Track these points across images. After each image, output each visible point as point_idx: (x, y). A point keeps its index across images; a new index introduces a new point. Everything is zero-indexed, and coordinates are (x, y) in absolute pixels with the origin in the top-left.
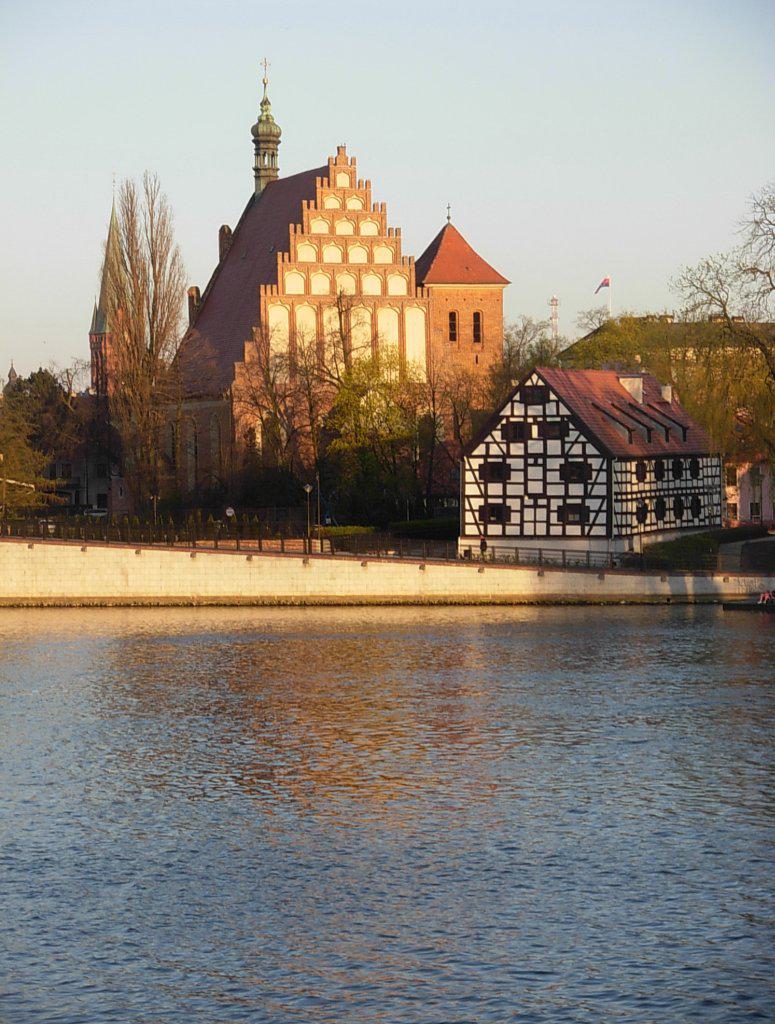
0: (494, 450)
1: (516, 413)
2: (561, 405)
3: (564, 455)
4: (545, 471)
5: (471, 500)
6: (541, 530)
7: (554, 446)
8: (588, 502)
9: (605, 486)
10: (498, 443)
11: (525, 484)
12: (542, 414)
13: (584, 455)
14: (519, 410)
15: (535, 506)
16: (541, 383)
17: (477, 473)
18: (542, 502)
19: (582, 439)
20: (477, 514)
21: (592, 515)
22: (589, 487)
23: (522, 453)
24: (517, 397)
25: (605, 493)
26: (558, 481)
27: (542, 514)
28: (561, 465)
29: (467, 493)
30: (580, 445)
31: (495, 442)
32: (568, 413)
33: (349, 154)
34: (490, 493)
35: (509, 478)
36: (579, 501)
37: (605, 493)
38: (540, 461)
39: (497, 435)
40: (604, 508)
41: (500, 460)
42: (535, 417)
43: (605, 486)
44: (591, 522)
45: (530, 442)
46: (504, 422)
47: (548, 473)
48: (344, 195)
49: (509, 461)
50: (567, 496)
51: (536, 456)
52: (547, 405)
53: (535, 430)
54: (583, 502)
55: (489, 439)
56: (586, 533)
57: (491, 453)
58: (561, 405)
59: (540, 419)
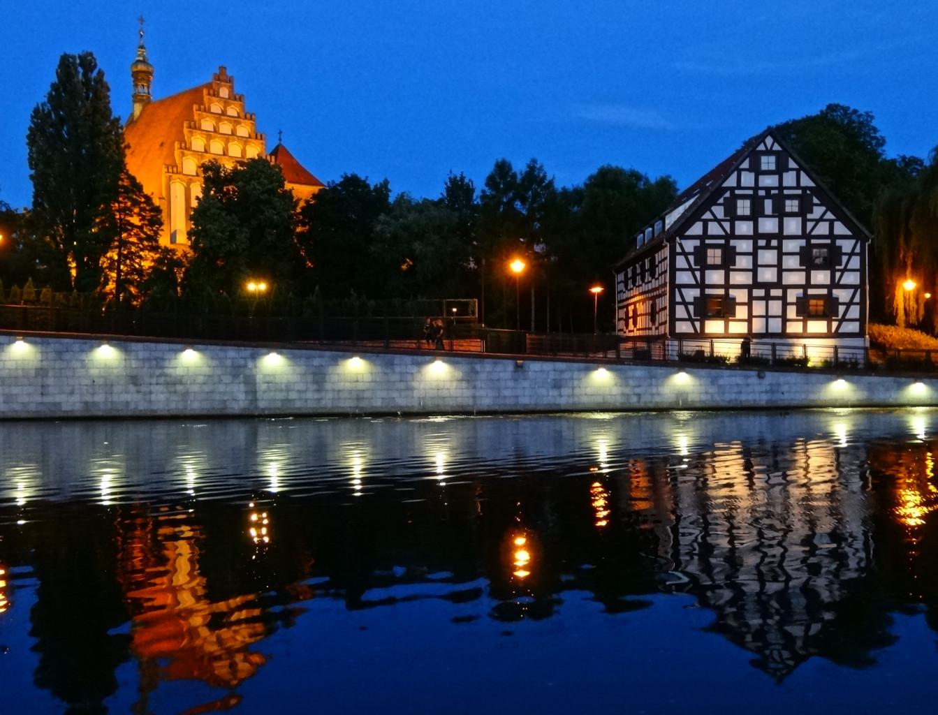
0: (714, 229)
1: (743, 185)
2: (802, 173)
3: (805, 235)
4: (781, 255)
5: (683, 290)
6: (775, 326)
7: (793, 226)
8: (836, 292)
9: (858, 273)
10: (719, 221)
11: (754, 272)
12: (777, 184)
13: (832, 236)
14: (748, 179)
15: (767, 298)
16: (777, 147)
17: (691, 258)
18: (776, 292)
19: (829, 216)
20: (691, 308)
21: (842, 309)
22: (838, 274)
23: (751, 233)
24: (746, 165)
25: (858, 282)
26: (798, 267)
27: (775, 307)
28: (801, 248)
29: (678, 282)
30: (826, 225)
31: (716, 219)
32: (812, 184)
33: (229, 73)
34: (707, 282)
35: (735, 265)
36: (824, 291)
37: (858, 282)
38: (774, 243)
39: (719, 211)
40: (857, 299)
41: (722, 242)
42: (768, 189)
43: (858, 273)
44: (840, 317)
45: (760, 220)
46: (728, 194)
47: (784, 257)
48: (226, 103)
49: (733, 243)
50: (808, 285)
51: (768, 237)
52: (785, 175)
53: (768, 206)
54: (830, 293)
55: (707, 215)
56: (833, 330)
57: (710, 232)
58: (802, 173)
59: (773, 192)
